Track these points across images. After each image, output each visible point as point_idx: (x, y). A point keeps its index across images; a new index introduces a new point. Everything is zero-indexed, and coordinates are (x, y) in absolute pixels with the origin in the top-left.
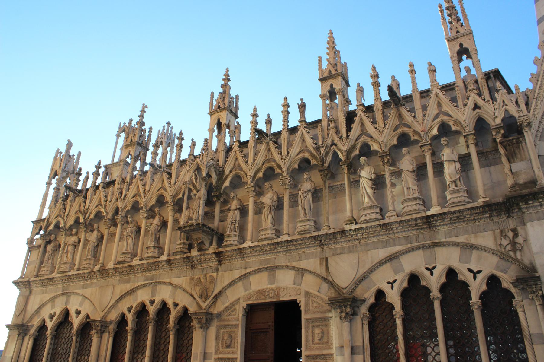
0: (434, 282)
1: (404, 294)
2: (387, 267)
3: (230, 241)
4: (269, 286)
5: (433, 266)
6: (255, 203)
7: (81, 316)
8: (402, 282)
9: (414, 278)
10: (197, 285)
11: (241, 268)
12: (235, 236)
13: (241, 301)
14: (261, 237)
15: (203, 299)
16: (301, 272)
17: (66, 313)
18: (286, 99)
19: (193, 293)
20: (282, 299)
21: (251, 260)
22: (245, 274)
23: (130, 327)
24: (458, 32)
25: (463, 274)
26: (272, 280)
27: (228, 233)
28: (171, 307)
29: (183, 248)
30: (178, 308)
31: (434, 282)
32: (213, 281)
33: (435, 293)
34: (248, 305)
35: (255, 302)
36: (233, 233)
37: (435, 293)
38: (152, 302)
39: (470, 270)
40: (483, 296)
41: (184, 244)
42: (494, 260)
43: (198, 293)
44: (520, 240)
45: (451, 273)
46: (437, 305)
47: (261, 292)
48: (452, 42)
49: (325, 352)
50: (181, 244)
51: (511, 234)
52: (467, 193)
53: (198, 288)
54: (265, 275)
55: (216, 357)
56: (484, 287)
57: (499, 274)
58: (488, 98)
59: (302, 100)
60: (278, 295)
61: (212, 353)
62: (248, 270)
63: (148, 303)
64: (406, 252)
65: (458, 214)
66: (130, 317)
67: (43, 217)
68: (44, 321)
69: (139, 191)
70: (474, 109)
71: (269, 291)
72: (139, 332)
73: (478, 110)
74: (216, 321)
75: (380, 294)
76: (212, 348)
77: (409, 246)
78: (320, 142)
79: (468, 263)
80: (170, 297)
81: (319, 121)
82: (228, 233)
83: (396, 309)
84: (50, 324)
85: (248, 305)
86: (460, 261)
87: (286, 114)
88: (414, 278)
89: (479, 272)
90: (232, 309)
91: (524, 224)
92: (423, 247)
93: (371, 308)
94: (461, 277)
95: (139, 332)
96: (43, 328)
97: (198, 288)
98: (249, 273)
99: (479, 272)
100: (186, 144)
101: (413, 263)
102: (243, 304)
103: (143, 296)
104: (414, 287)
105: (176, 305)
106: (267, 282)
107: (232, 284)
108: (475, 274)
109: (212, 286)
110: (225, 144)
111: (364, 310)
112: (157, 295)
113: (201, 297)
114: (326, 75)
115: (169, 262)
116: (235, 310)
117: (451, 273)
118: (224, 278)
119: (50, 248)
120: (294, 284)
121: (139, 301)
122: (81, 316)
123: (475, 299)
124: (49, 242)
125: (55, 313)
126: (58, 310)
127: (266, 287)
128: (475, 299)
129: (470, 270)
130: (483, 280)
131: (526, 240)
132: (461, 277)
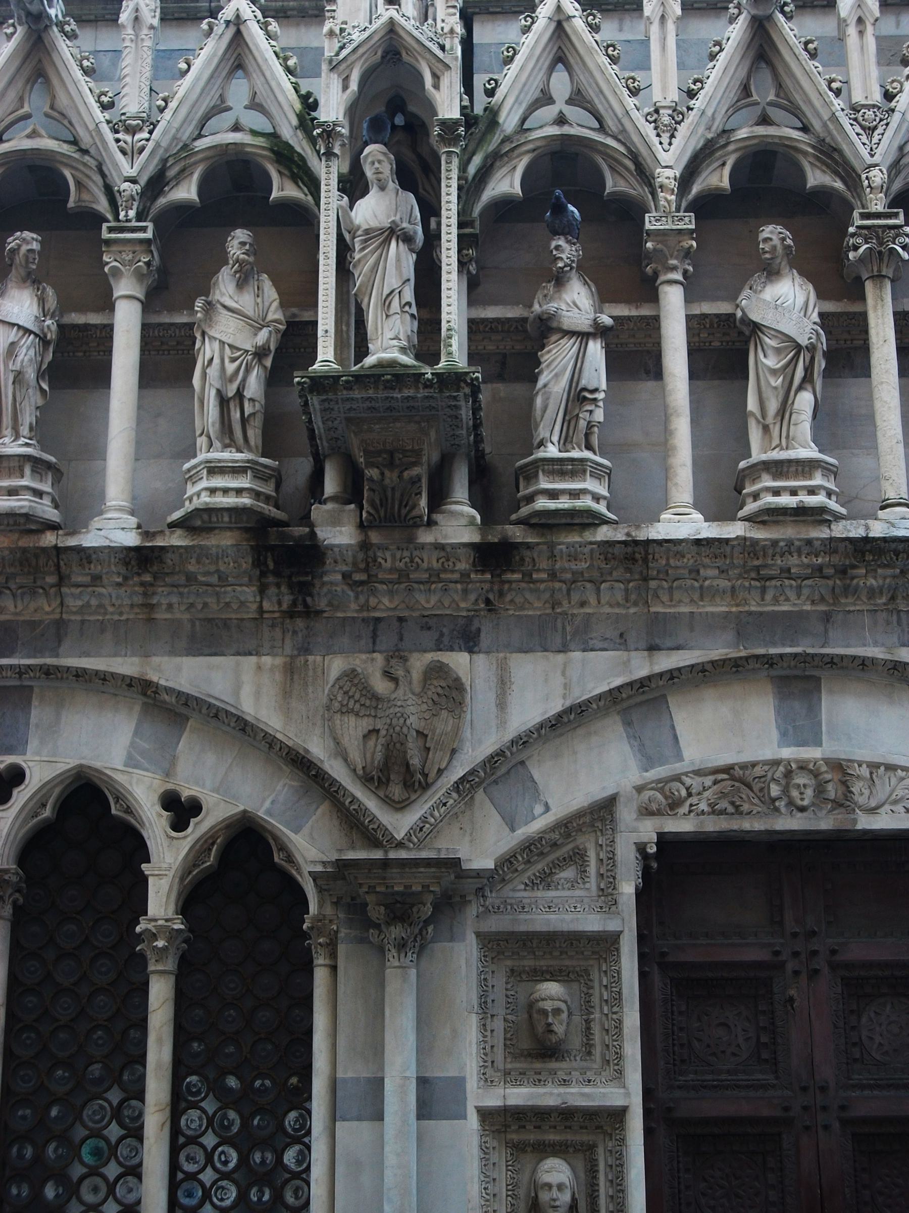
3: (575, 494)
4: (787, 753)
10: (345, 711)
11: (622, 642)
13: (626, 814)
15: (396, 791)
19: (318, 749)
20: (865, 822)
21: (685, 609)
22: (649, 678)
26: (801, 726)
27: (552, 451)
28: (154, 823)
29: (257, 495)
30: (198, 828)
32: (450, 693)
34: (663, 840)
35: (712, 825)
41: (259, 473)
43: (355, 756)
47: (736, 778)
50: (236, 470)
53: (353, 729)
55: (493, 1099)
60: (844, 803)
61: (460, 1083)
62: (667, 662)
71: (788, 774)
74: (472, 910)
76: (466, 1056)
80: (131, 762)
85: (663, 840)
90: (560, 853)
97: (353, 729)
98: (672, 675)
102: (637, 831)
105: (180, 810)
106: (775, 735)
109: (443, 724)
112: (33, 744)
113: (374, 779)
115: (141, 559)
116: (578, 858)
118: (517, 689)
127: (768, 754)
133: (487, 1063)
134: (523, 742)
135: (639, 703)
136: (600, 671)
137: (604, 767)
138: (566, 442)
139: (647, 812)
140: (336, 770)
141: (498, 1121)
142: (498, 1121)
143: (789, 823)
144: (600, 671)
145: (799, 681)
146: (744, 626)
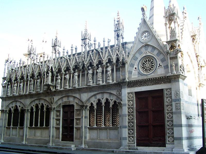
0: (103, 102)
1: (97, 104)
2: (93, 97)
5: (104, 98)
6: (64, 77)
7: (21, 107)
8: (96, 101)
9: (99, 100)
12: (59, 87)
13: (61, 104)
14: (65, 88)
16: (75, 97)
17: (16, 106)
18: (72, 45)
20: (70, 104)
23: (34, 110)
24: (118, 29)
25: (109, 100)
27: (57, 86)
31: (103, 102)
33: (103, 104)
36: (59, 86)
37: (103, 104)
38: (39, 104)
39: (111, 99)
40: (113, 106)
42: (116, 97)
44: (121, 93)
45: (107, 99)
46: (103, 107)
48: (115, 32)
49: (79, 117)
51: (119, 91)
52: (112, 80)
54: (67, 98)
56: (113, 104)
57: (116, 101)
58: (120, 53)
59: (76, 46)
63: (38, 104)
64: (98, 94)
65: (109, 85)
66: (34, 108)
67: (5, 77)
68: (10, 108)
69: (33, 71)
70: (117, 56)
72: (37, 112)
73: (117, 56)
75: (92, 104)
77: (98, 92)
78: (80, 61)
79: (110, 97)
81: (81, 53)
82: (57, 86)
83: (95, 108)
84: (12, 110)
86: (109, 97)
87: (72, 50)
88: (99, 100)
89: (112, 100)
91: (122, 89)
92: (102, 93)
93: (90, 107)
94: (109, 101)
95: (37, 112)
96: (10, 111)
99: (112, 100)
100: (46, 57)
101: (99, 97)
102: (62, 105)
103: (37, 102)
104: (99, 103)
107: (59, 99)
108: (112, 100)
110: (57, 57)
111: (88, 108)
114: (83, 38)
117: (107, 99)
119: (9, 86)
120: (73, 100)
121: (36, 103)
122: (21, 107)
123: (111, 106)
124: (8, 85)
125: (13, 106)
126: (14, 106)
128: (111, 106)
129: (111, 99)
130: (113, 102)
131: (122, 93)
132: (109, 101)
133: (56, 116)
134: (57, 101)
135: (62, 98)
136: (60, 97)
137: (60, 102)
138: (58, 85)
139: (62, 104)
140: (49, 102)
141: (56, 119)
142: (56, 119)
143: (67, 104)
144: (60, 97)
145: (68, 96)
146: (66, 94)
